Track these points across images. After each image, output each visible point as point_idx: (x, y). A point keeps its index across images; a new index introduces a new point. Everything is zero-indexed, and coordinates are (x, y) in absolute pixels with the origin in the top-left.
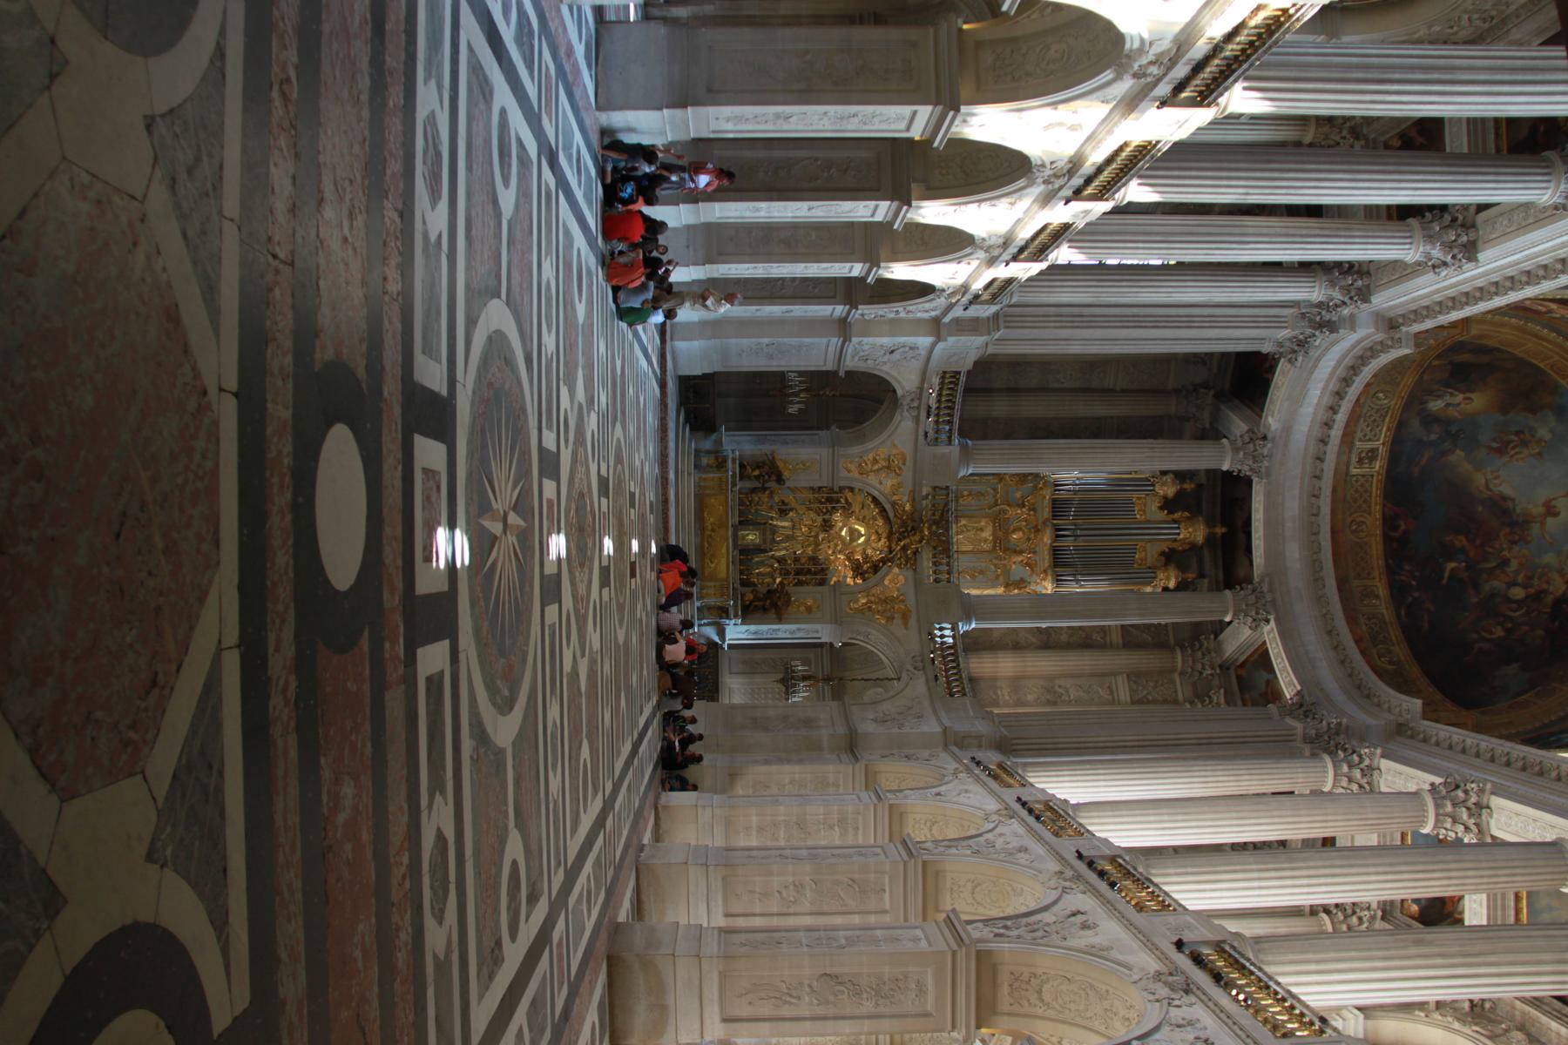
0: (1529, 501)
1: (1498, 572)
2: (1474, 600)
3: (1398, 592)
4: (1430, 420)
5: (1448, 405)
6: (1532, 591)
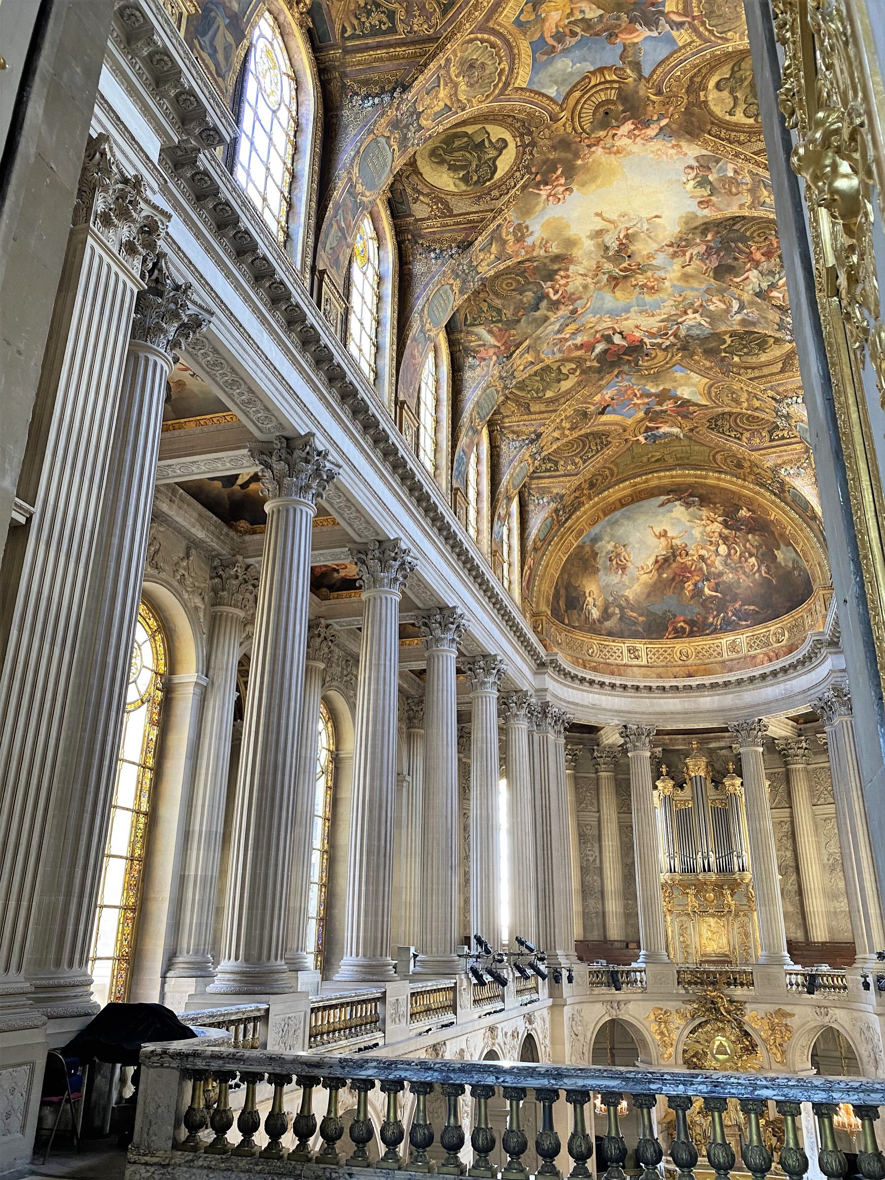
0: (660, 548)
1: (709, 562)
2: (731, 575)
3: (728, 626)
4: (606, 615)
5: (595, 605)
6: (721, 541)
